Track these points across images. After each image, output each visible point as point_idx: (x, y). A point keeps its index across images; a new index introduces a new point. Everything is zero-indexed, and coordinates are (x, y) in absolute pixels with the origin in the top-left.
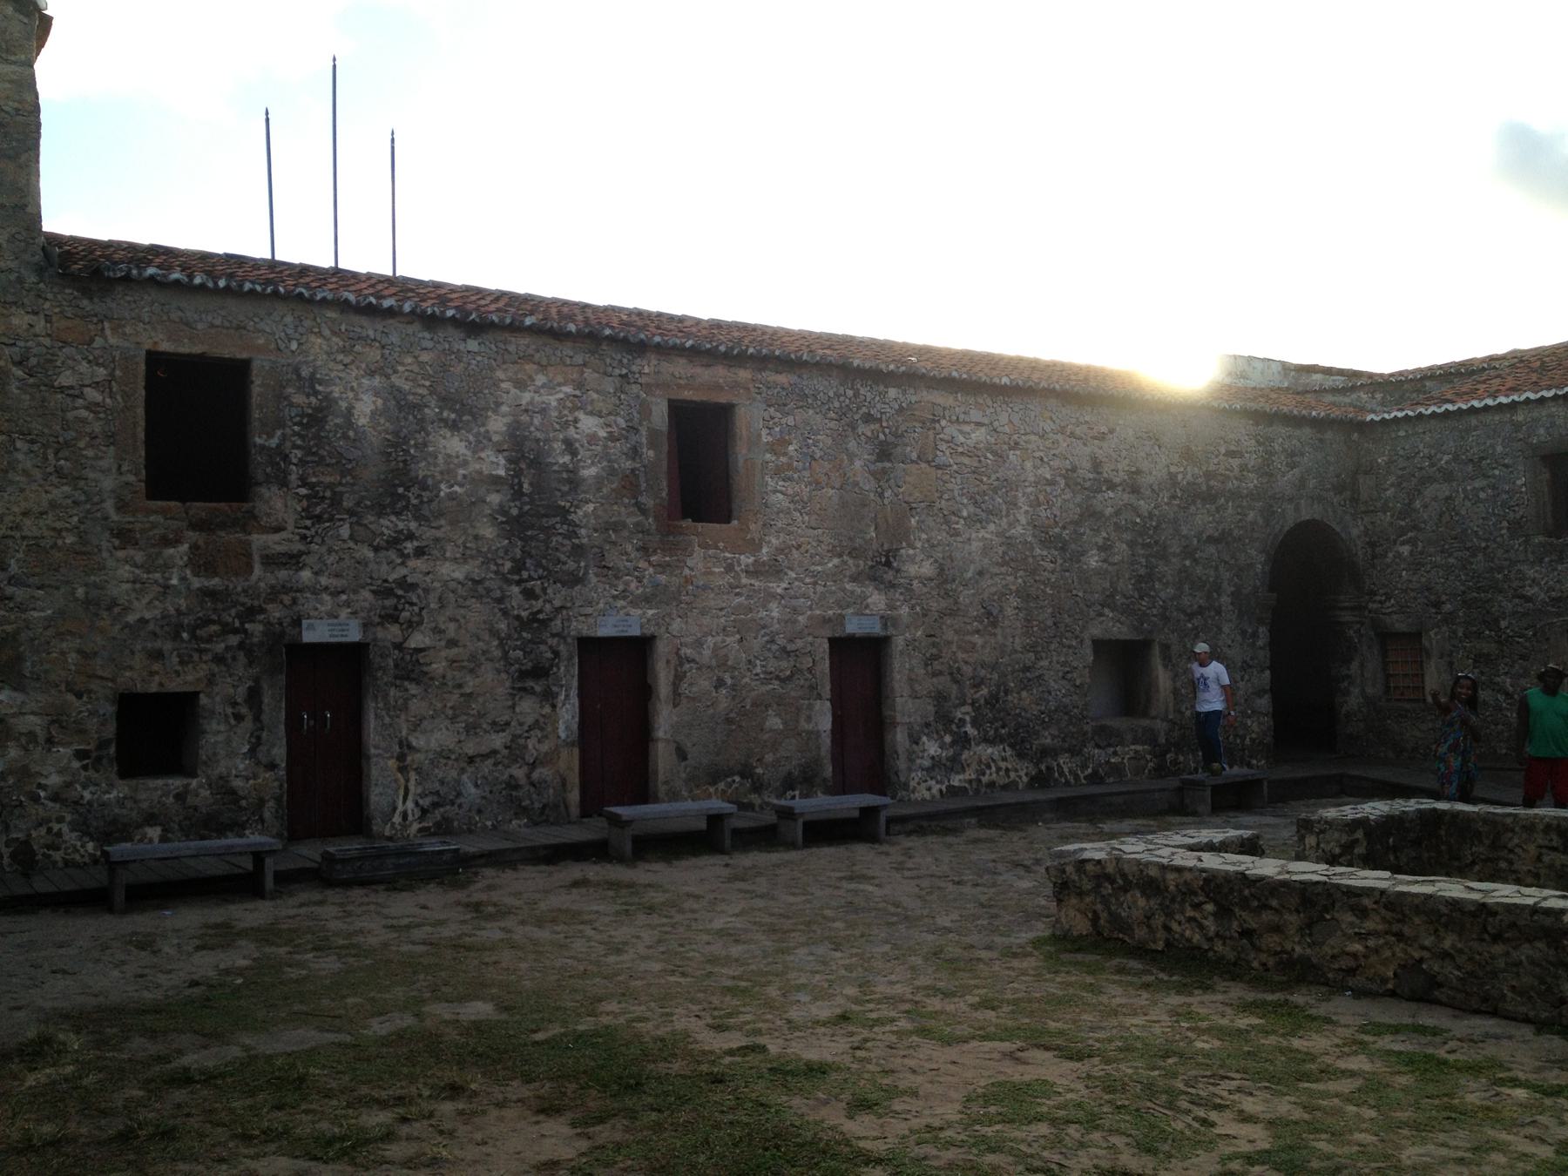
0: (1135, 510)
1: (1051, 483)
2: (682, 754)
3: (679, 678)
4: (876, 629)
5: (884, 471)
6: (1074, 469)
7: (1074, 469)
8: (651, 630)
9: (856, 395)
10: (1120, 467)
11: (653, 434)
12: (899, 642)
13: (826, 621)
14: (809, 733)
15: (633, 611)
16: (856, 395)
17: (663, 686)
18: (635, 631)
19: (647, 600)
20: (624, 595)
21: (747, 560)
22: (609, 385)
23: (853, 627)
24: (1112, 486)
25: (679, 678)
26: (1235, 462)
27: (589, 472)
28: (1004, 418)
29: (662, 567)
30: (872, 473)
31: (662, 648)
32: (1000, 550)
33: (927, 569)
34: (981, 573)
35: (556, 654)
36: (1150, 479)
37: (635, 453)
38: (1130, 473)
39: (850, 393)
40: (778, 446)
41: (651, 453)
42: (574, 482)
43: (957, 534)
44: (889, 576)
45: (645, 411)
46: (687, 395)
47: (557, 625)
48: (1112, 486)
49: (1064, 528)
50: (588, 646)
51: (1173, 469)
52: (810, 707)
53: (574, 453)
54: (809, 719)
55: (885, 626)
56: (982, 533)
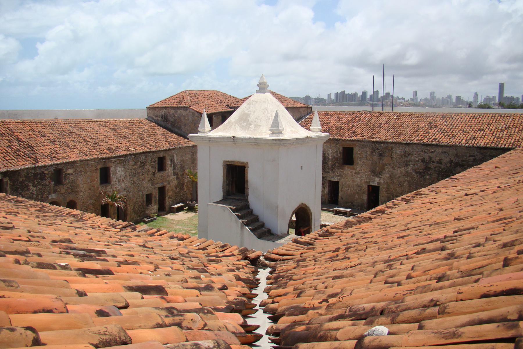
0: (440, 167)
1: (418, 161)
2: (342, 198)
3: (342, 188)
4: (376, 185)
5: (380, 158)
6: (424, 158)
7: (424, 158)
8: (338, 181)
9: (375, 145)
10: (436, 158)
11: (340, 153)
12: (381, 187)
13: (367, 182)
14: (363, 199)
15: (336, 177)
16: (375, 145)
17: (340, 189)
18: (336, 180)
19: (338, 176)
20: (335, 175)
21: (354, 171)
22: (334, 145)
23: (371, 184)
24: (434, 162)
25: (342, 188)
26: (472, 158)
27: (330, 158)
28: (407, 149)
29: (341, 172)
30: (379, 158)
31: (340, 183)
32: (404, 173)
33: (388, 175)
34: (399, 177)
35: (325, 182)
36: (444, 161)
37: (337, 155)
38: (439, 160)
39: (374, 145)
40: (360, 154)
41: (340, 155)
42: (329, 159)
43: (395, 169)
44: (380, 176)
45: (339, 149)
46: (346, 146)
47: (326, 178)
48: (434, 162)
49: (420, 170)
50: (330, 181)
51: (451, 159)
52: (363, 195)
53: (329, 155)
54: (363, 197)
55: (378, 184)
56: (400, 170)
